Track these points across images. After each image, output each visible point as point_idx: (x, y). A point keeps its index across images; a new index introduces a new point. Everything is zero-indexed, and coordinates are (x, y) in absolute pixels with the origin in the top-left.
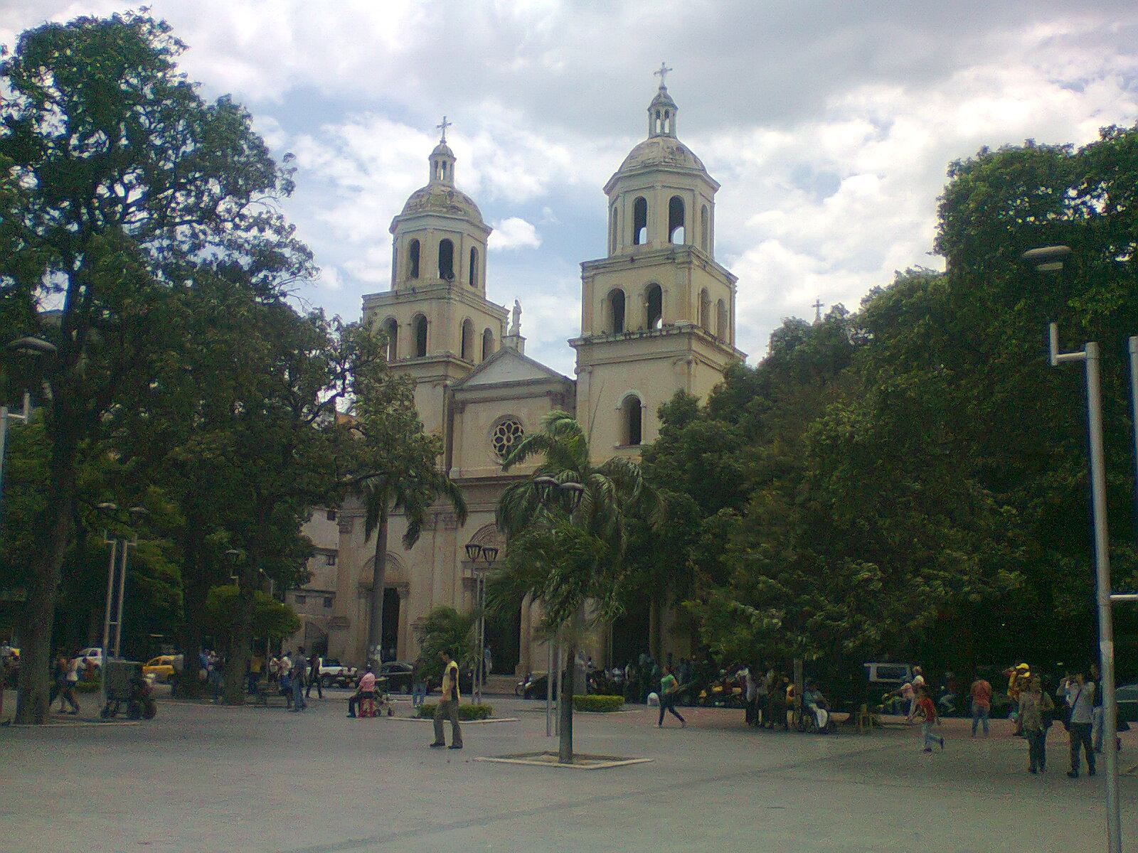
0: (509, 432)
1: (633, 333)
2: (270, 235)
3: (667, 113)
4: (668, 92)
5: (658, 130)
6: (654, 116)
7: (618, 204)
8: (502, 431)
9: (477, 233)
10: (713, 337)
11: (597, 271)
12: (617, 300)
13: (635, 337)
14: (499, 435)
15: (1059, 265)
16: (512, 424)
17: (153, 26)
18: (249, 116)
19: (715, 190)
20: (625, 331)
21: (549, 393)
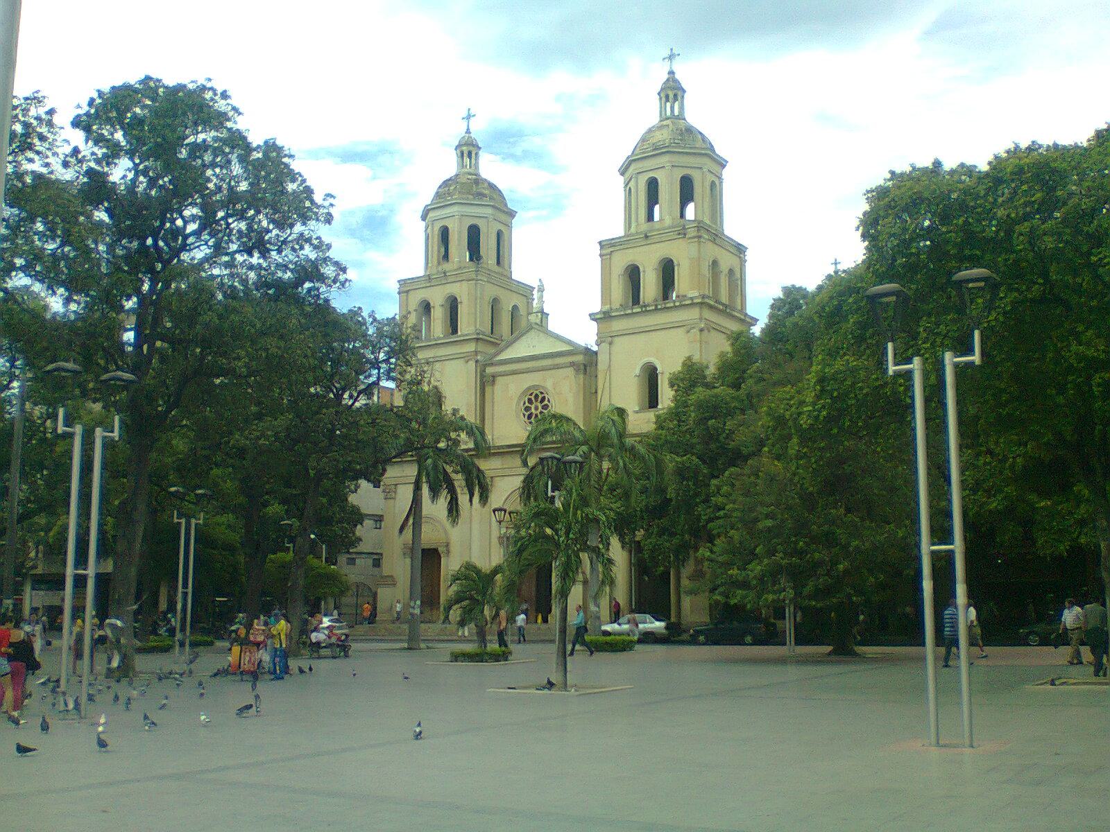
0: (536, 401)
1: (648, 305)
2: (309, 252)
3: (675, 96)
4: (677, 76)
5: (669, 113)
6: (664, 99)
7: (632, 184)
8: (530, 401)
9: (503, 217)
10: (723, 304)
12: (633, 274)
13: (651, 308)
14: (527, 404)
15: (893, 298)
17: (215, 94)
18: (291, 156)
19: (723, 166)
21: (572, 364)
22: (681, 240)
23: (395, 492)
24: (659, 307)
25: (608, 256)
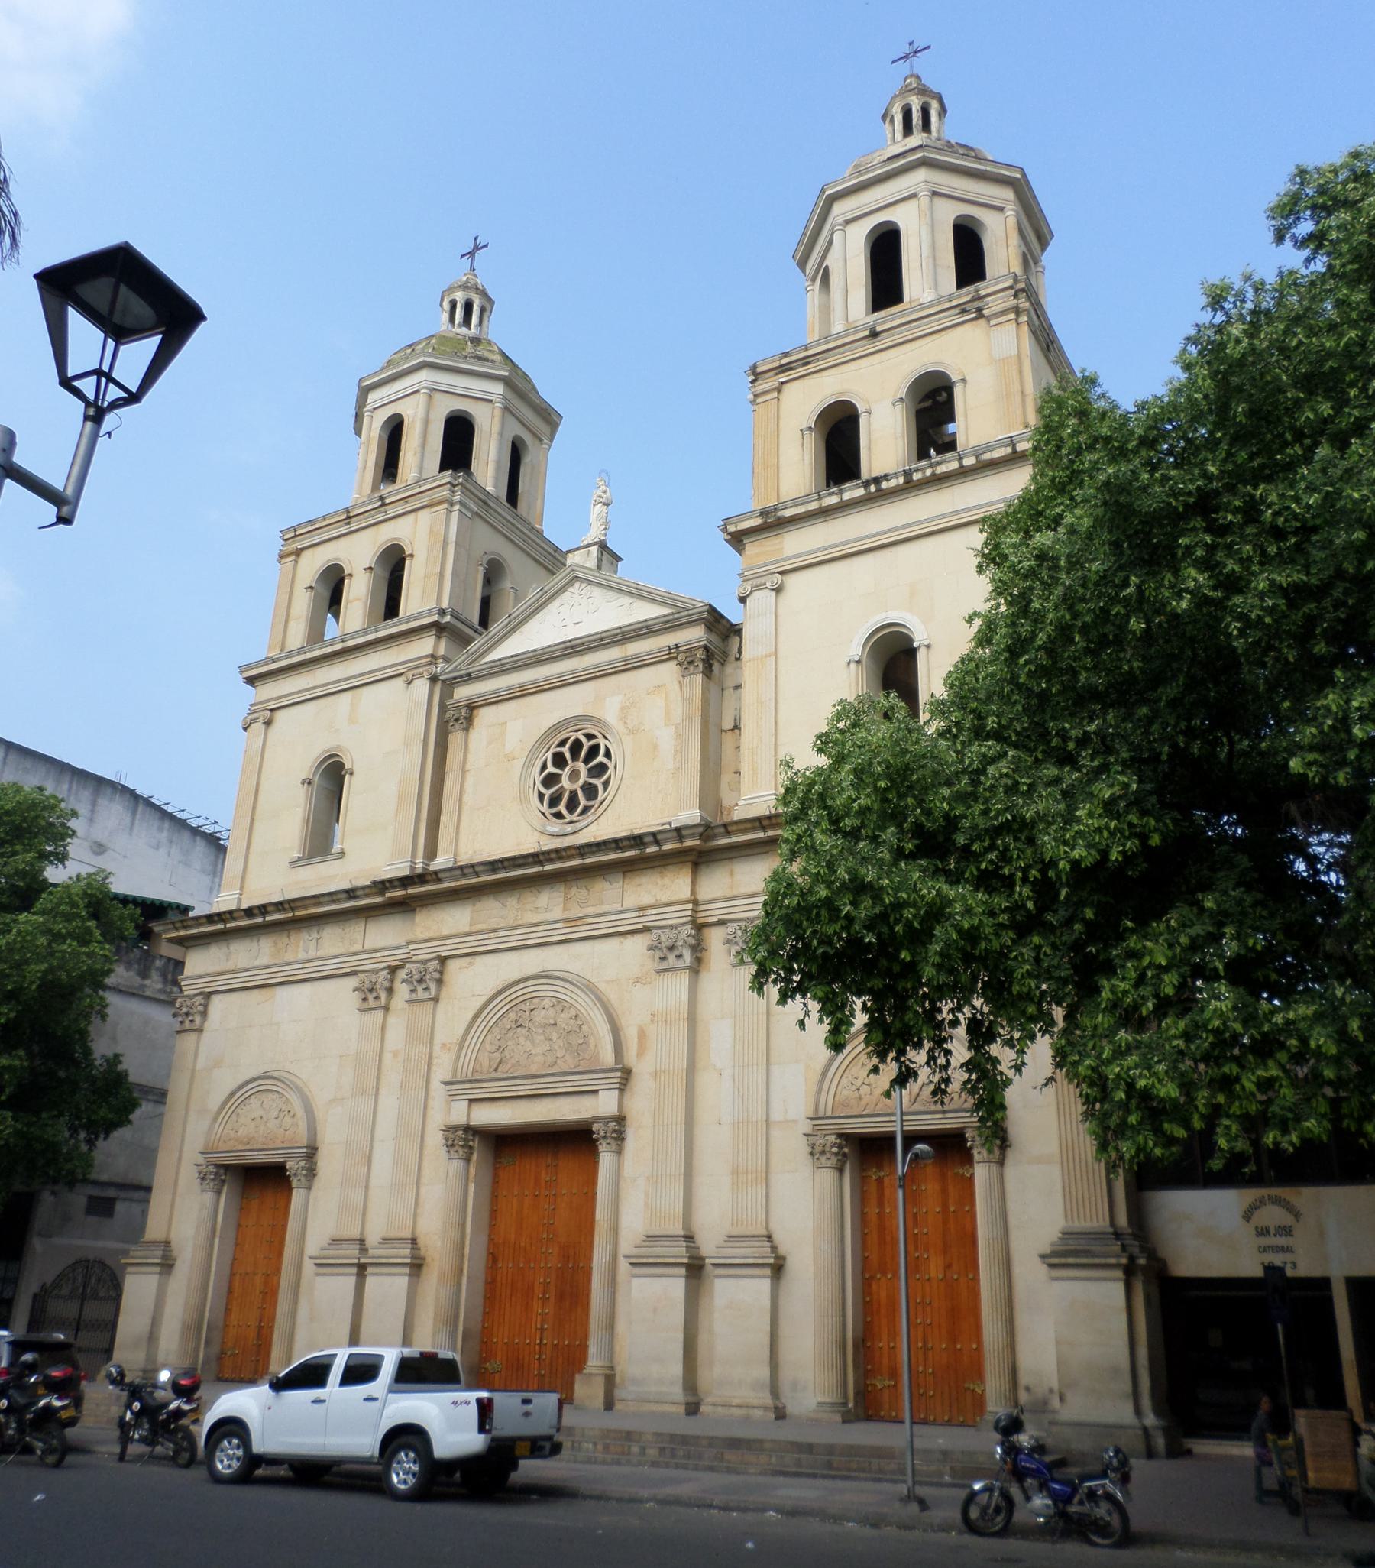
8: (559, 760)
11: (783, 378)
13: (893, 483)
14: (551, 769)
16: (583, 739)
20: (865, 474)
21: (672, 654)
22: (966, 326)
23: (204, 1014)
24: (916, 476)
25: (775, 394)
